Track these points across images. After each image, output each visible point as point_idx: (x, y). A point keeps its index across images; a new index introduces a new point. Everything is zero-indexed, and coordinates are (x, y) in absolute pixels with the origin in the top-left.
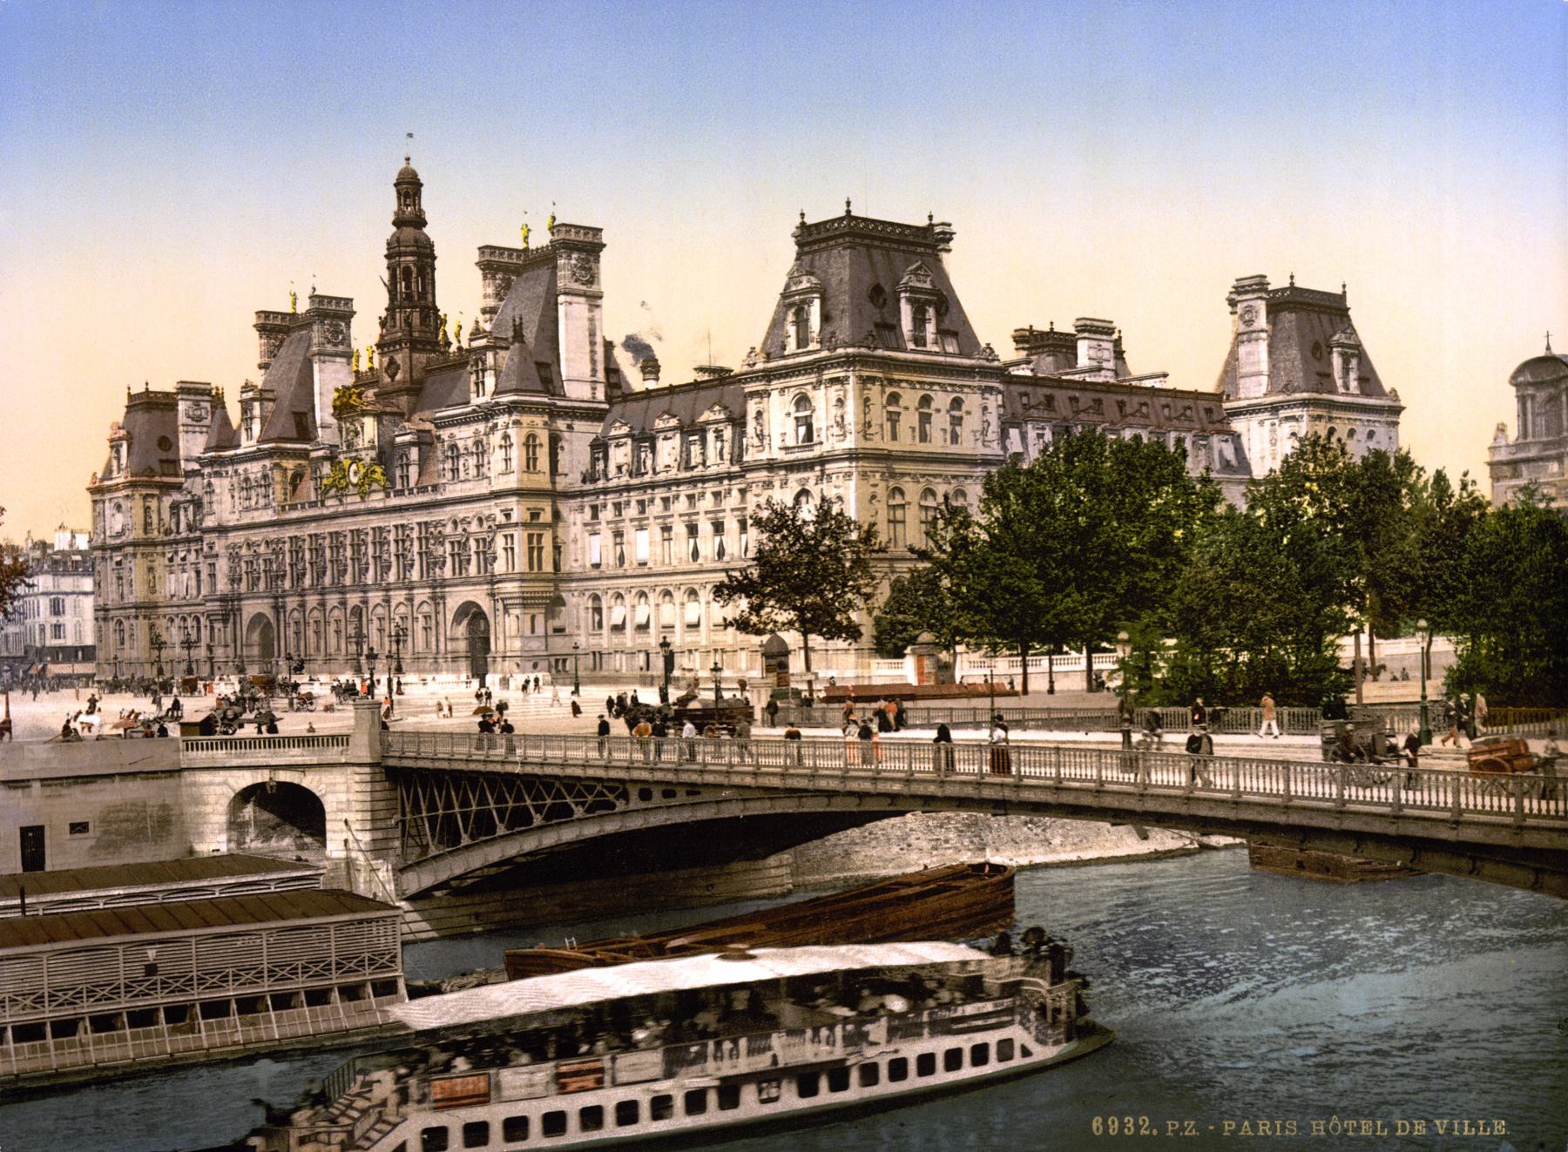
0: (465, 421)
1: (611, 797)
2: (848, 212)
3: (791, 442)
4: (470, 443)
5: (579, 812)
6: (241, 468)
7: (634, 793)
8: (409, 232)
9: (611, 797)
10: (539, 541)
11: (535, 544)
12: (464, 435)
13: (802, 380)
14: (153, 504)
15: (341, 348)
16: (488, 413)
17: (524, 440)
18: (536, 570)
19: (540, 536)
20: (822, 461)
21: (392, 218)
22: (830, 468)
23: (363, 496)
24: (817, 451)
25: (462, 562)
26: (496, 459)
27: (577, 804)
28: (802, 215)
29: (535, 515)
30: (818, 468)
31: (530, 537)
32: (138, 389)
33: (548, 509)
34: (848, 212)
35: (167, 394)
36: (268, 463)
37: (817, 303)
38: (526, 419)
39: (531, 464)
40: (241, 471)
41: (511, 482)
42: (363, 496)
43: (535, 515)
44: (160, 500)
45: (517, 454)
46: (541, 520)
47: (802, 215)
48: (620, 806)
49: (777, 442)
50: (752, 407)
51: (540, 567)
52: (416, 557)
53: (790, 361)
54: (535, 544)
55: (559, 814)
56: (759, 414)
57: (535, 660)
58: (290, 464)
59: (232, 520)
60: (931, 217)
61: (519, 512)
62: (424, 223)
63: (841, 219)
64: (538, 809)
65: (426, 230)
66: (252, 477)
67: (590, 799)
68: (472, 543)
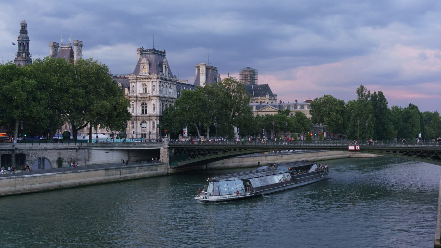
1: (217, 151)
3: (141, 92)
7: (232, 150)
8: (24, 35)
9: (217, 151)
13: (145, 80)
20: (149, 97)
21: (19, 31)
22: (151, 98)
24: (148, 95)
30: (148, 99)
49: (138, 92)
50: (131, 85)
53: (141, 76)
56: (134, 86)
65: (27, 34)
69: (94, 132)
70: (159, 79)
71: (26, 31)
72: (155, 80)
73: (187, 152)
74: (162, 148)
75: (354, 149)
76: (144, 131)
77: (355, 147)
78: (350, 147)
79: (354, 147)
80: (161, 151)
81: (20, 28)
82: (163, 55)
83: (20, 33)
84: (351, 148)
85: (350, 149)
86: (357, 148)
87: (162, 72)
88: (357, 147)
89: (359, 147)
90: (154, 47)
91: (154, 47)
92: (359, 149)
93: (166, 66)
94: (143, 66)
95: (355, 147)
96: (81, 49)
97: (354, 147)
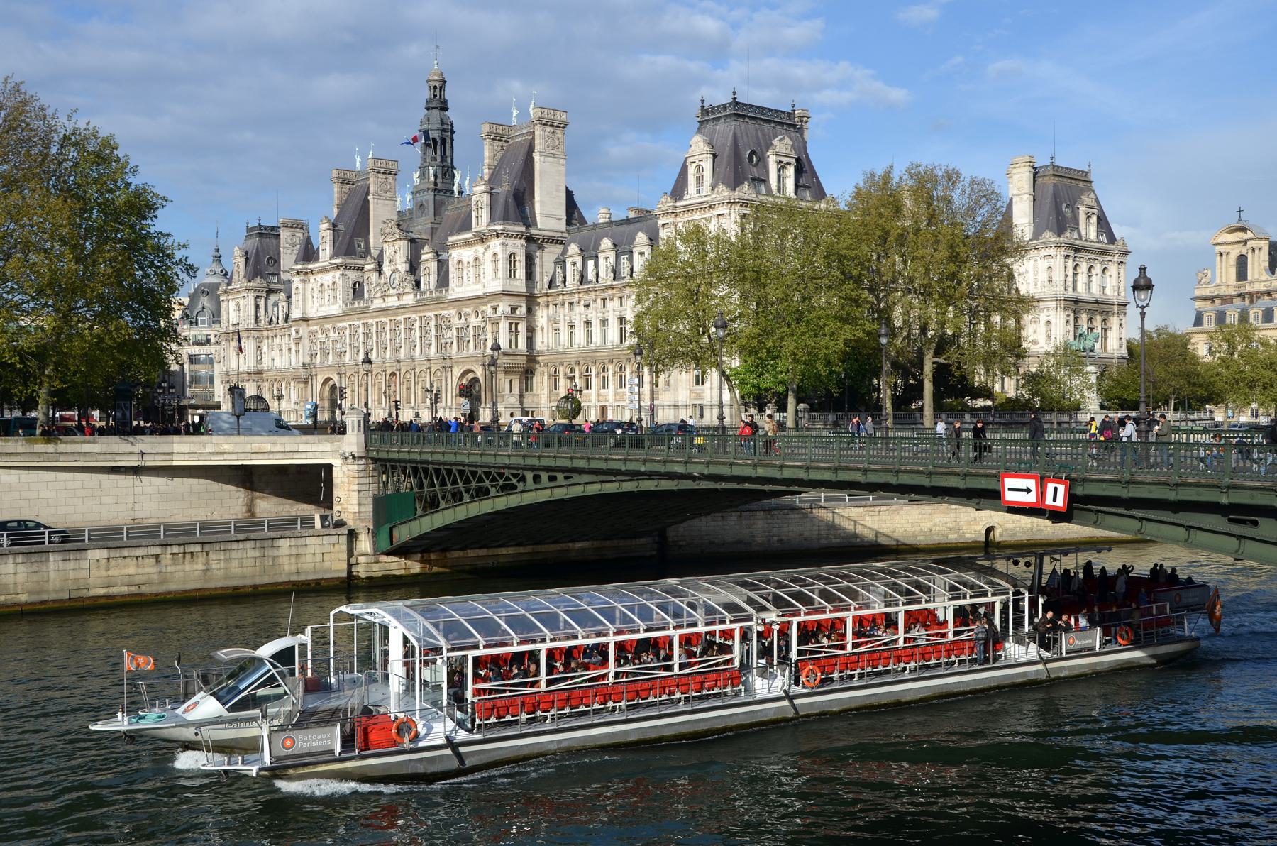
0: (467, 244)
2: (735, 98)
4: (471, 260)
5: (493, 492)
6: (318, 277)
9: (514, 481)
10: (516, 329)
11: (513, 329)
12: (467, 254)
14: (262, 303)
15: (388, 194)
16: (482, 239)
17: (507, 256)
18: (513, 347)
19: (517, 324)
23: (399, 296)
25: (463, 342)
26: (487, 267)
27: (492, 486)
28: (703, 101)
29: (513, 310)
31: (510, 324)
32: (254, 224)
33: (524, 305)
34: (735, 98)
35: (273, 228)
36: (338, 273)
37: (710, 161)
38: (510, 242)
39: (512, 273)
40: (318, 279)
41: (497, 286)
42: (399, 296)
43: (513, 310)
44: (266, 299)
45: (502, 265)
46: (518, 312)
47: (703, 101)
48: (521, 486)
51: (516, 347)
52: (433, 339)
54: (513, 329)
55: (482, 493)
57: (512, 410)
58: (353, 275)
59: (312, 313)
60: (793, 105)
61: (504, 307)
62: (446, 109)
63: (730, 104)
64: (467, 491)
66: (326, 284)
67: (501, 482)
68: (471, 328)
69: (616, 400)
70: (738, 207)
71: (445, 102)
72: (724, 210)
73: (461, 480)
74: (337, 463)
75: (1031, 498)
76: (699, 396)
77: (1042, 495)
78: (1009, 483)
79: (1031, 484)
80: (339, 476)
81: (427, 94)
82: (782, 124)
83: (428, 109)
84: (1018, 489)
85: (1010, 497)
86: (1049, 501)
87: (764, 181)
88: (1050, 487)
89: (1061, 489)
90: (734, 93)
91: (734, 93)
92: (1060, 502)
93: (786, 160)
94: (694, 165)
95: (1042, 495)
96: (560, 136)
97: (1031, 484)
